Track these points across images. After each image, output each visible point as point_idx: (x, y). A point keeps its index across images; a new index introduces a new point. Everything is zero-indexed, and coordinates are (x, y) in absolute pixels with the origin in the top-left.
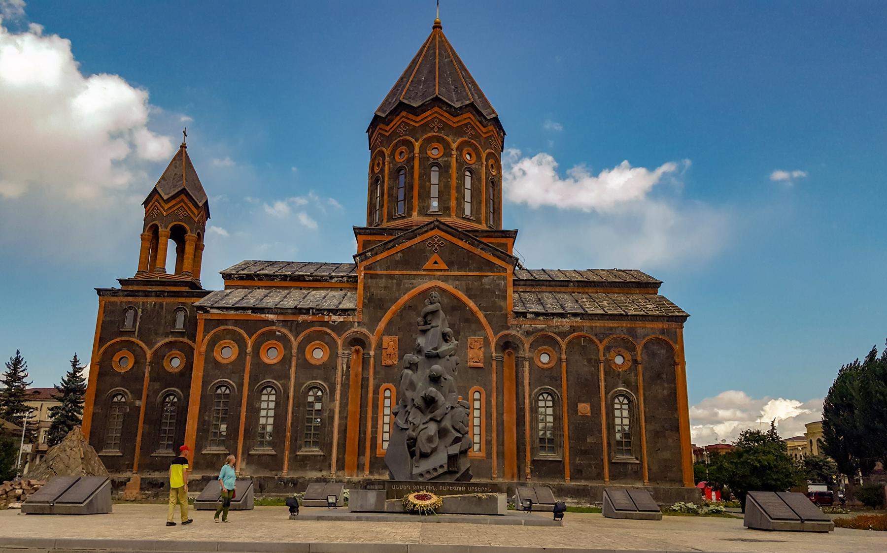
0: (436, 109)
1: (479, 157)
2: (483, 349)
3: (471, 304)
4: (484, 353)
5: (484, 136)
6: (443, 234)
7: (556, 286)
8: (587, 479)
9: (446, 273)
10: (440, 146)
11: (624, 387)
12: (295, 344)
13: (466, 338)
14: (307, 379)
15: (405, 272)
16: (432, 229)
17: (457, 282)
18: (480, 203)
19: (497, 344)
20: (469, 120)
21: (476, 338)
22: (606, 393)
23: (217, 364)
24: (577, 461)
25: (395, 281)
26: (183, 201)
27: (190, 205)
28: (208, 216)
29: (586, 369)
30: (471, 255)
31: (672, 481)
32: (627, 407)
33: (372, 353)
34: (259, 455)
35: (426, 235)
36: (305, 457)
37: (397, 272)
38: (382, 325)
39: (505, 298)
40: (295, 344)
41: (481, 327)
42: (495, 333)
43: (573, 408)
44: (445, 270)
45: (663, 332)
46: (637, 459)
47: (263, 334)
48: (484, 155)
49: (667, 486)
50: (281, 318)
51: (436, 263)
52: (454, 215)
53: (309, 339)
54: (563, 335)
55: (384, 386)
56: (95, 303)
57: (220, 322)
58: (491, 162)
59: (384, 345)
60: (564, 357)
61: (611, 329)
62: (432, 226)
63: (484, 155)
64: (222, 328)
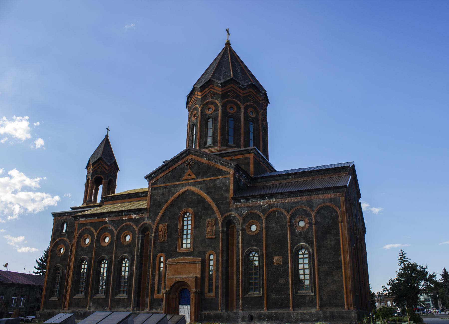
0: (211, 86)
1: (239, 108)
2: (214, 227)
3: (208, 198)
4: (216, 228)
5: (242, 95)
6: (194, 157)
7: (281, 179)
8: (278, 308)
9: (195, 180)
10: (213, 106)
11: (304, 242)
12: (116, 233)
13: (205, 219)
14: (121, 254)
15: (173, 183)
16: (188, 155)
17: (201, 185)
18: (240, 135)
19: (223, 221)
20: (232, 88)
21: (210, 220)
22: (292, 248)
23: (82, 249)
24: (273, 296)
25: (167, 190)
26: (101, 164)
27: (104, 165)
28: (118, 170)
29: (279, 233)
30: (209, 167)
31: (337, 306)
32: (307, 256)
33: (153, 235)
34: (99, 299)
35: (184, 159)
36: (120, 300)
37: (168, 184)
38: (159, 217)
39: (228, 191)
40: (116, 233)
41: (214, 213)
42: (222, 216)
43: (270, 259)
44: (195, 179)
45: (331, 200)
46: (312, 292)
47: (102, 229)
48: (242, 107)
49: (334, 310)
50: (111, 219)
51: (189, 175)
52: (219, 145)
53: (123, 229)
54: (264, 211)
55: (160, 254)
56: (51, 221)
57: (85, 224)
58: (249, 110)
59: (160, 229)
60: (264, 226)
61: (296, 203)
62: (187, 153)
63: (242, 107)
64: (84, 228)
